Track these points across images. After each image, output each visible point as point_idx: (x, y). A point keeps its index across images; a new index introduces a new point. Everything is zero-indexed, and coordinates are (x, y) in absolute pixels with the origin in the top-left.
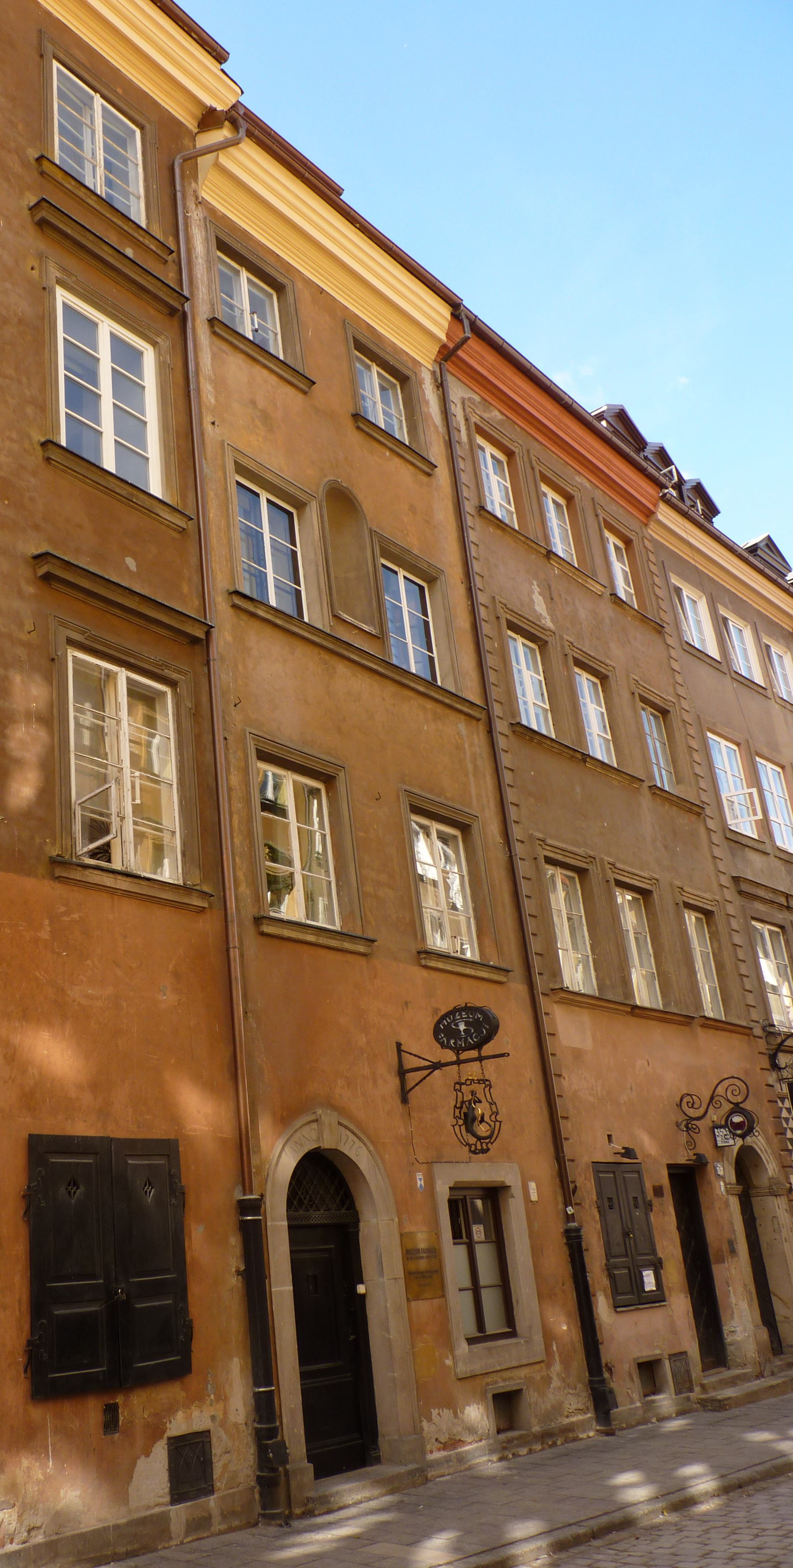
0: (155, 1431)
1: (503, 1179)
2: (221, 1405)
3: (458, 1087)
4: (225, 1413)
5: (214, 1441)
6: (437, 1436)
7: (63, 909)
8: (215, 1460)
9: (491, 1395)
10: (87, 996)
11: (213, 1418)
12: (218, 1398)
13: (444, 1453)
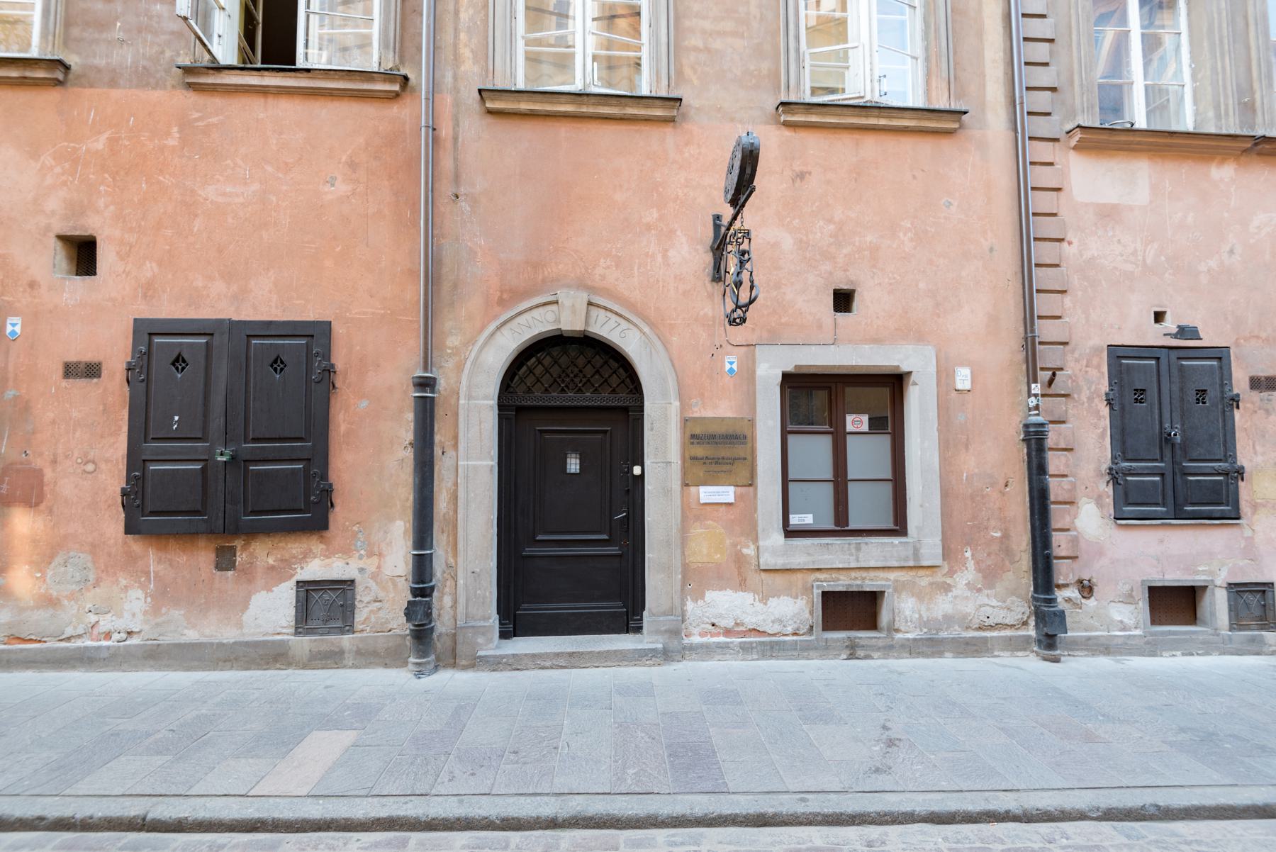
0: (277, 573)
2: (375, 560)
4: (379, 567)
5: (359, 589)
6: (714, 621)
7: (196, 115)
9: (820, 591)
10: (224, 194)
11: (361, 570)
12: (370, 554)
13: (722, 639)
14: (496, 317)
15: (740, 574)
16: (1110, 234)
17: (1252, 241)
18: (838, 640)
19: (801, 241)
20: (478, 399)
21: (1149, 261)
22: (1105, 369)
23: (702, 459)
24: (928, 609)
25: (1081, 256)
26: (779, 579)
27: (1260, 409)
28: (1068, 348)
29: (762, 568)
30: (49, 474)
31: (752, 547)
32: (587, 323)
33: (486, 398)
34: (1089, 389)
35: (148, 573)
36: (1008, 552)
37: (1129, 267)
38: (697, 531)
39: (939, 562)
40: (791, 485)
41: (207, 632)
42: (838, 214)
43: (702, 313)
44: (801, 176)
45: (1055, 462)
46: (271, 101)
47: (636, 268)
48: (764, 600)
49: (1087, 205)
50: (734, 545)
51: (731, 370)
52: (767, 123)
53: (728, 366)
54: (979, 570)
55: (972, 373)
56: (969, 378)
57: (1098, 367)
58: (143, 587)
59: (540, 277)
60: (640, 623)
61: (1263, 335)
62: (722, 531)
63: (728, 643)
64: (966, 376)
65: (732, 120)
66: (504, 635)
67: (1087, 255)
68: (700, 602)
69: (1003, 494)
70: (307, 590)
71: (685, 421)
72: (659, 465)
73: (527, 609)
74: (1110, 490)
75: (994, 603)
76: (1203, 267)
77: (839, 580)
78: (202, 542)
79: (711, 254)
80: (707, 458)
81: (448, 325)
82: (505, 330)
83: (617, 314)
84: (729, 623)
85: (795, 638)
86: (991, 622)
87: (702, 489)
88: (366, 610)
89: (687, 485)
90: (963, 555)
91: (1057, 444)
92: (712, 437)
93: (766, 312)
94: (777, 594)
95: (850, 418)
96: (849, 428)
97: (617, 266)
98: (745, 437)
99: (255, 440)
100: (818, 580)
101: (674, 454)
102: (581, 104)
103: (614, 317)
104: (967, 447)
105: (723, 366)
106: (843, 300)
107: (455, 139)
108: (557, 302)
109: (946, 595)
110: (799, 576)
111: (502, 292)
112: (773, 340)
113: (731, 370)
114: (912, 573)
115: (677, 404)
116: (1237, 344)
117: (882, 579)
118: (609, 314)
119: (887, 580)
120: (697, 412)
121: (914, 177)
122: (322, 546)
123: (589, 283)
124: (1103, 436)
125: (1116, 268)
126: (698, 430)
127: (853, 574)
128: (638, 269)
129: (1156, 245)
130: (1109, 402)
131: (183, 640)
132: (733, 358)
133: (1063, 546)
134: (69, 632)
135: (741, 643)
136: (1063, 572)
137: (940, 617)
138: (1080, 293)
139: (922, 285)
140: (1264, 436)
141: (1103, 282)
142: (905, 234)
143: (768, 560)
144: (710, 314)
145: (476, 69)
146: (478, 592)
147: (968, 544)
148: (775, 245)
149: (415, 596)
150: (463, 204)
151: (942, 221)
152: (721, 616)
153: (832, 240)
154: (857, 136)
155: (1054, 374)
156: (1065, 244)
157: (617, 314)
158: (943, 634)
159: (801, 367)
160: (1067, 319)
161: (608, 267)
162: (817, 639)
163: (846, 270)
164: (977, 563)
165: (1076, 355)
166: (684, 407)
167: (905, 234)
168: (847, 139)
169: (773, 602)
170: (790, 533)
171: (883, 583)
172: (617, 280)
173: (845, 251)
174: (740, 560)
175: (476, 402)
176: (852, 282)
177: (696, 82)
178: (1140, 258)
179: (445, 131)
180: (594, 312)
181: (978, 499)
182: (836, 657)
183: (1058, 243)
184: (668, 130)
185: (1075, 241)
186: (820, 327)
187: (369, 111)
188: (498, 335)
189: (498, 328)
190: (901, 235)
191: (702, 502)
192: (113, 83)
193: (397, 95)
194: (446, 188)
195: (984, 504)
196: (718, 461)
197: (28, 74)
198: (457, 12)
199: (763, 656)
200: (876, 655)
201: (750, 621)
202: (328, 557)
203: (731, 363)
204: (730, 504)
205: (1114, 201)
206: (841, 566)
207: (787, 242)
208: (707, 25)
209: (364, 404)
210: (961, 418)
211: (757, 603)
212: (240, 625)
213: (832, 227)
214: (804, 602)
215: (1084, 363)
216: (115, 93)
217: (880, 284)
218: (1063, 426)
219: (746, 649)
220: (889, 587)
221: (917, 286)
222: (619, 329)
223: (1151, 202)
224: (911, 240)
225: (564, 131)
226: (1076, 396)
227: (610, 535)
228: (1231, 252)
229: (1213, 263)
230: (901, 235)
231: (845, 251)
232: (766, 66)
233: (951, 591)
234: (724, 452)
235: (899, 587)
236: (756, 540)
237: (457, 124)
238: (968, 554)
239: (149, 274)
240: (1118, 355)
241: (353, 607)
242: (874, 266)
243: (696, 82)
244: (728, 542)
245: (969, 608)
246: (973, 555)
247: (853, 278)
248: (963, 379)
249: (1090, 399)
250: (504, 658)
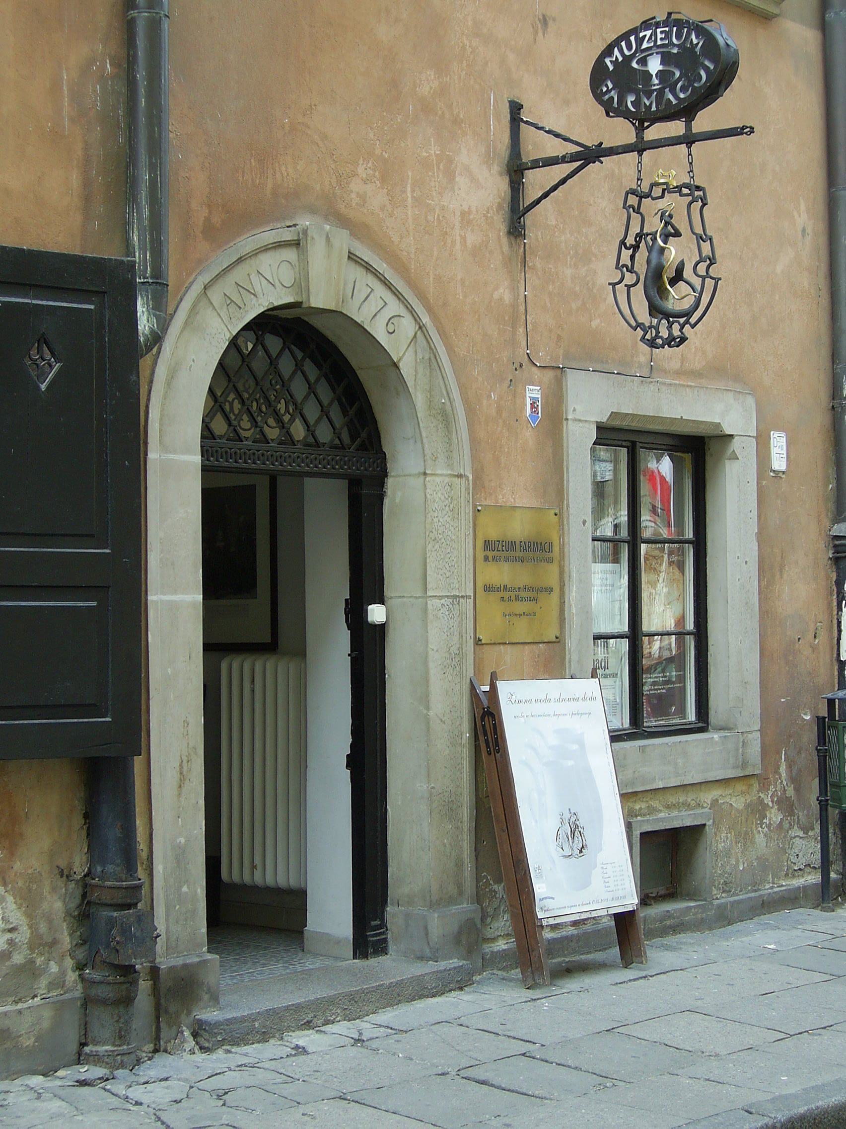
1: (717, 421)
3: (633, 200)
9: (638, 833)
20: (175, 452)
23: (499, 589)
33: (188, 451)
43: (496, 295)
47: (409, 189)
59: (270, 185)
60: (383, 933)
72: (443, 601)
77: (652, 810)
79: (507, 179)
92: (511, 545)
93: (574, 306)
103: (380, 290)
118: (371, 280)
123: (342, 208)
127: (672, 799)
128: (413, 191)
146: (185, 889)
172: (382, 208)
175: (172, 456)
250: (255, 1020)
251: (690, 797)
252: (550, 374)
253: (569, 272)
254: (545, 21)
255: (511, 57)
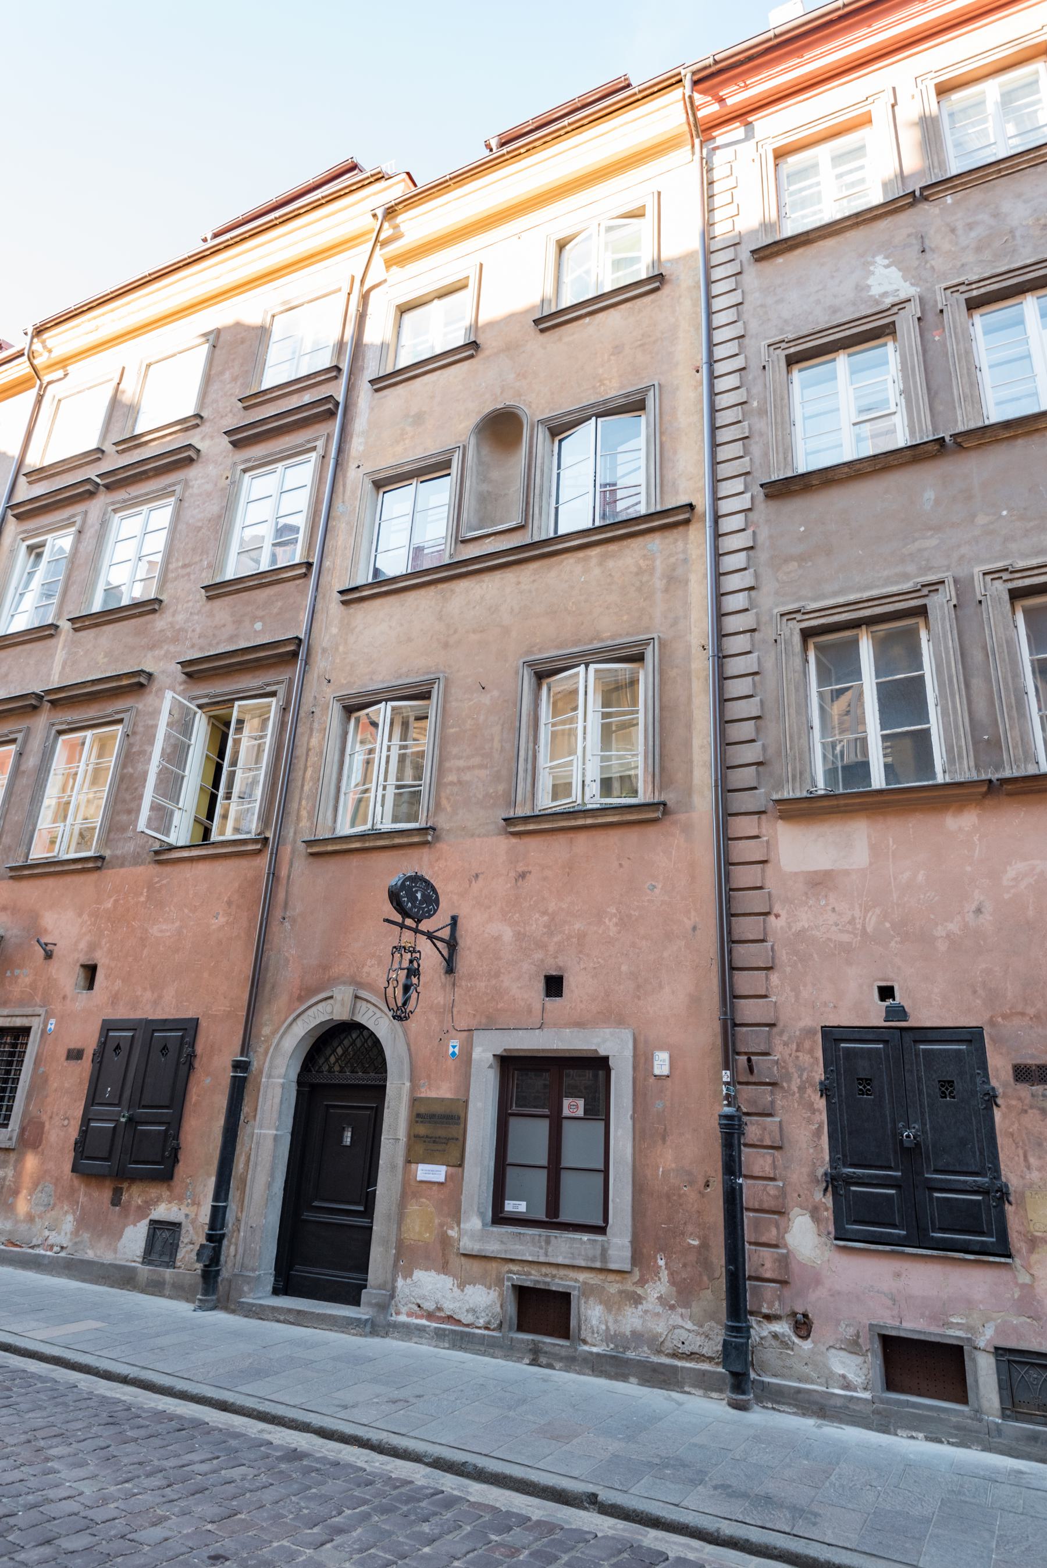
1: (594, 1048)
5: (183, 1231)
6: (419, 1301)
8: (181, 1245)
11: (187, 1216)
12: (193, 1204)
13: (424, 1322)
14: (295, 1010)
15: (444, 1255)
16: (823, 903)
17: (1006, 896)
18: (522, 1341)
19: (519, 933)
21: (869, 929)
22: (819, 1054)
24: (616, 1321)
25: (790, 928)
26: (476, 1267)
27: (1031, 1107)
28: (775, 1030)
29: (462, 1251)
30: (47, 1125)
31: (456, 1229)
32: (353, 1011)
34: (800, 1077)
35: (78, 1203)
36: (706, 1264)
37: (846, 938)
38: (413, 1207)
39: (627, 1267)
40: (510, 1172)
41: (99, 1253)
42: (552, 906)
44: (523, 875)
45: (755, 1161)
46: (194, 864)
48: (461, 1286)
49: (796, 873)
50: (441, 1225)
51: (454, 1053)
52: (500, 834)
53: (451, 1050)
54: (673, 1282)
55: (670, 1057)
56: (667, 1062)
57: (811, 1051)
58: (74, 1213)
61: (1031, 1011)
62: (433, 1209)
63: (425, 1326)
64: (664, 1061)
65: (473, 835)
66: (276, 1292)
67: (797, 927)
68: (409, 1281)
69: (702, 1195)
70: (157, 1226)
71: (414, 1101)
73: (301, 1271)
74: (829, 1201)
75: (689, 1325)
76: (940, 932)
78: (108, 1183)
80: (427, 1137)
81: (266, 1017)
82: (299, 1022)
83: (374, 1005)
84: (430, 1306)
85: (486, 1332)
86: (686, 1349)
87: (421, 1167)
88: (184, 1250)
89: (409, 1162)
90: (656, 1262)
91: (762, 1140)
94: (473, 1282)
95: (566, 1102)
96: (566, 1112)
97: (379, 964)
98: (459, 1118)
99: (144, 1107)
100: (510, 1272)
101: (402, 1133)
102: (364, 841)
103: (372, 1008)
104: (664, 1140)
105: (447, 1050)
106: (554, 985)
107: (289, 877)
108: (331, 997)
109: (636, 1308)
110: (494, 1265)
111: (301, 990)
112: (490, 1024)
113: (454, 1053)
114: (601, 1277)
115: (408, 1084)
116: (992, 1022)
117: (571, 1279)
118: (369, 1005)
119: (576, 1281)
120: (425, 1093)
121: (621, 865)
122: (168, 1193)
123: (358, 979)
124: (818, 1133)
125: (829, 939)
126: (422, 1110)
127: (544, 1270)
129: (878, 911)
130: (825, 1090)
131: (86, 1257)
132: (456, 1042)
133: (768, 1265)
134: (35, 1242)
135: (436, 1328)
136: (768, 1299)
137: (628, 1333)
138: (788, 969)
139: (624, 968)
140: (1040, 1145)
141: (815, 956)
142: (610, 920)
143: (468, 1244)
144: (442, 1002)
145: (308, 824)
147: (661, 1250)
148: (497, 939)
149: (208, 1240)
150: (287, 925)
151: (646, 904)
152: (424, 1298)
153: (545, 930)
154: (571, 835)
155: (749, 1060)
156: (772, 918)
157: (374, 1005)
158: (630, 1355)
159: (510, 1050)
160: (774, 999)
161: (372, 966)
162: (503, 1337)
163: (555, 958)
164: (672, 1274)
165: (785, 1038)
166: (413, 1088)
167: (610, 920)
168: (562, 839)
169: (469, 1289)
170: (499, 1218)
171: (572, 1283)
172: (377, 975)
173: (555, 939)
174: (445, 1241)
176: (560, 968)
177: (449, 809)
178: (859, 926)
179: (284, 873)
180: (359, 1003)
181: (675, 1198)
182: (519, 1360)
183: (762, 917)
184: (425, 850)
185: (783, 914)
186: (530, 1011)
187: (244, 863)
188: (294, 1024)
189: (295, 1020)
190: (607, 921)
191: (418, 1179)
192: (122, 865)
193: (260, 851)
194: (278, 913)
195: (681, 1205)
196: (435, 1140)
197: (86, 866)
198: (303, 786)
199: (453, 1346)
200: (558, 1365)
201: (449, 1307)
202: (170, 1202)
203: (454, 1047)
204: (441, 1184)
205: (828, 866)
206: (530, 1259)
207: (508, 934)
208: (461, 763)
209: (208, 1080)
210: (659, 1105)
211: (455, 1289)
212: (115, 1251)
213: (546, 918)
214: (497, 1293)
215: (794, 1046)
216: (123, 871)
217: (585, 969)
218: (769, 1119)
219: (440, 1334)
220: (574, 1288)
221: (620, 968)
222: (374, 1018)
223: (871, 864)
224: (616, 924)
225: (355, 861)
226: (785, 1085)
227: (366, 1208)
228: (979, 911)
229: (953, 927)
230: (607, 921)
231: (555, 939)
232: (501, 788)
233: (641, 1303)
234: (441, 1132)
235: (588, 1291)
236: (459, 1225)
237: (291, 866)
238: (662, 1263)
239: (116, 988)
240: (832, 1036)
241: (178, 1246)
242: (581, 952)
243: (449, 809)
244: (437, 1221)
245: (660, 1327)
246: (666, 1264)
247: (561, 964)
248: (661, 1063)
249: (802, 1089)
251: (572, 1274)
252: (465, 1034)
253: (483, 984)
254: (477, 876)
255: (455, 897)
